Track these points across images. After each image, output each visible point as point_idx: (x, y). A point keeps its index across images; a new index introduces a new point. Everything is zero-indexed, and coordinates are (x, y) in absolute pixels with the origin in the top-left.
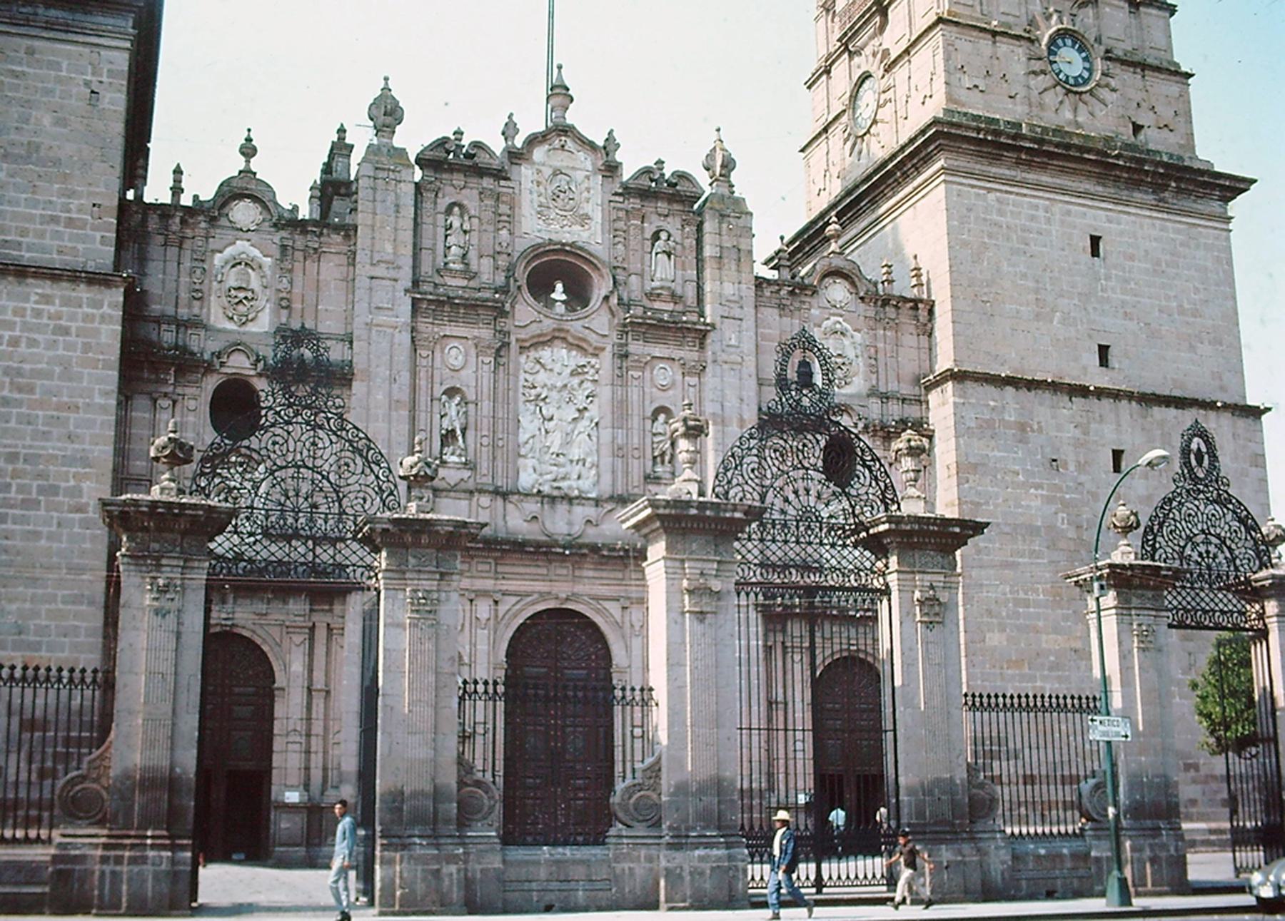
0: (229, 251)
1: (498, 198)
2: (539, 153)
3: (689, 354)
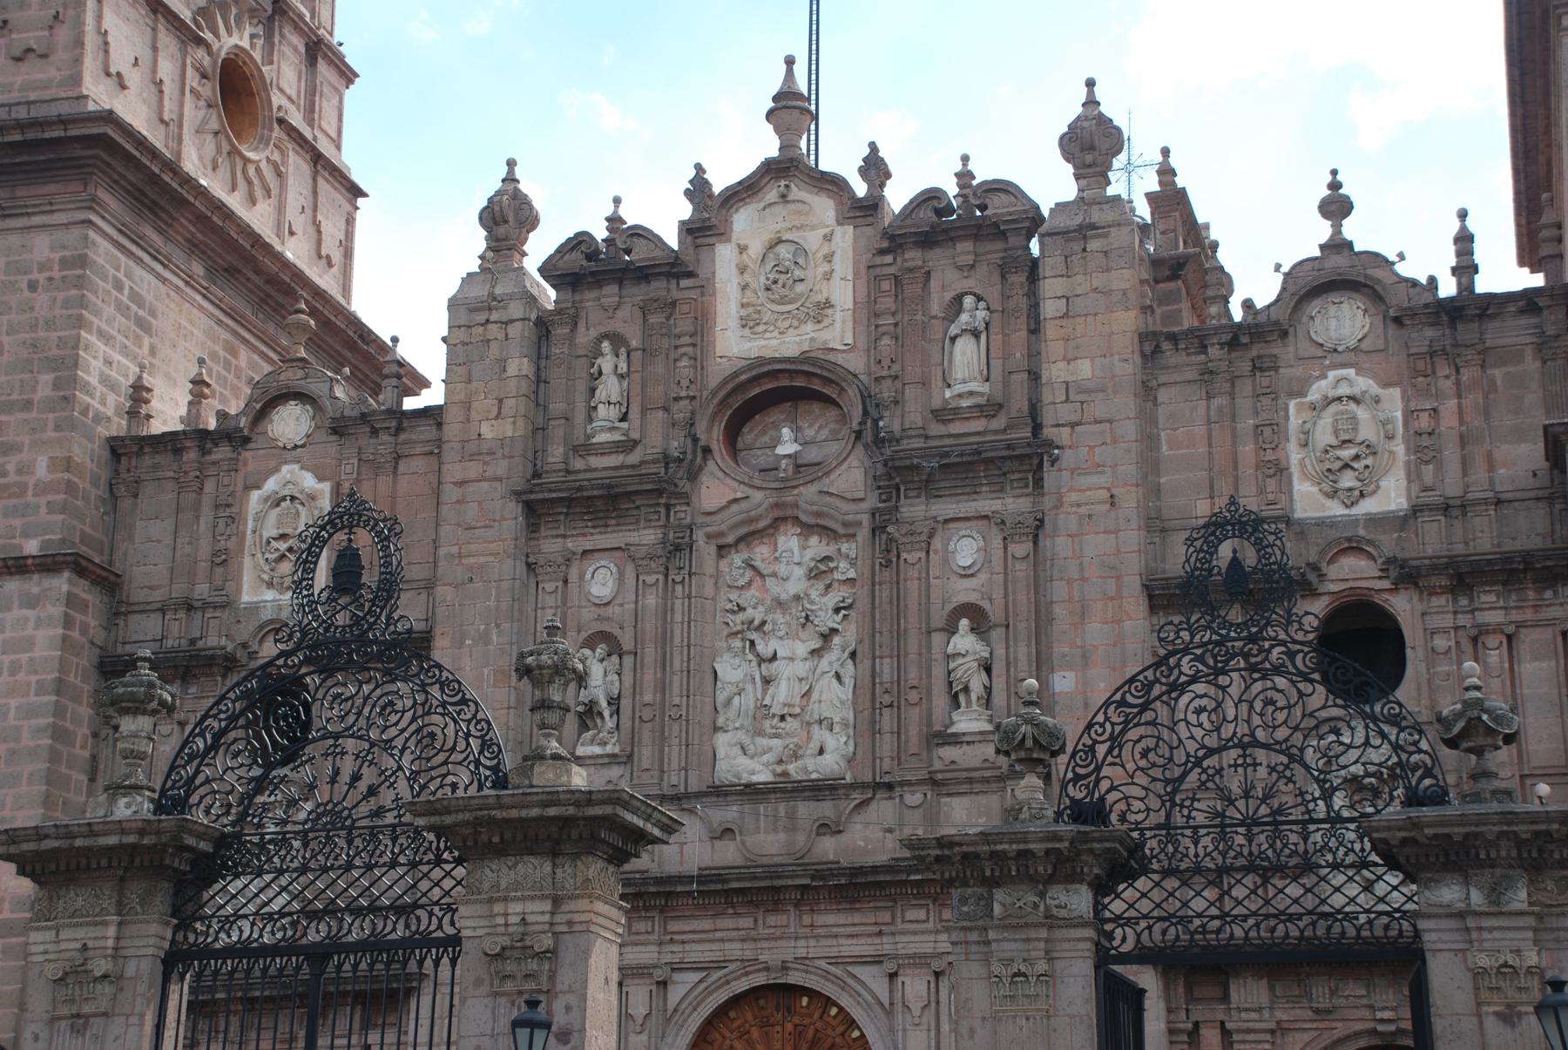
0: (271, 485)
2: (743, 221)
3: (1014, 504)
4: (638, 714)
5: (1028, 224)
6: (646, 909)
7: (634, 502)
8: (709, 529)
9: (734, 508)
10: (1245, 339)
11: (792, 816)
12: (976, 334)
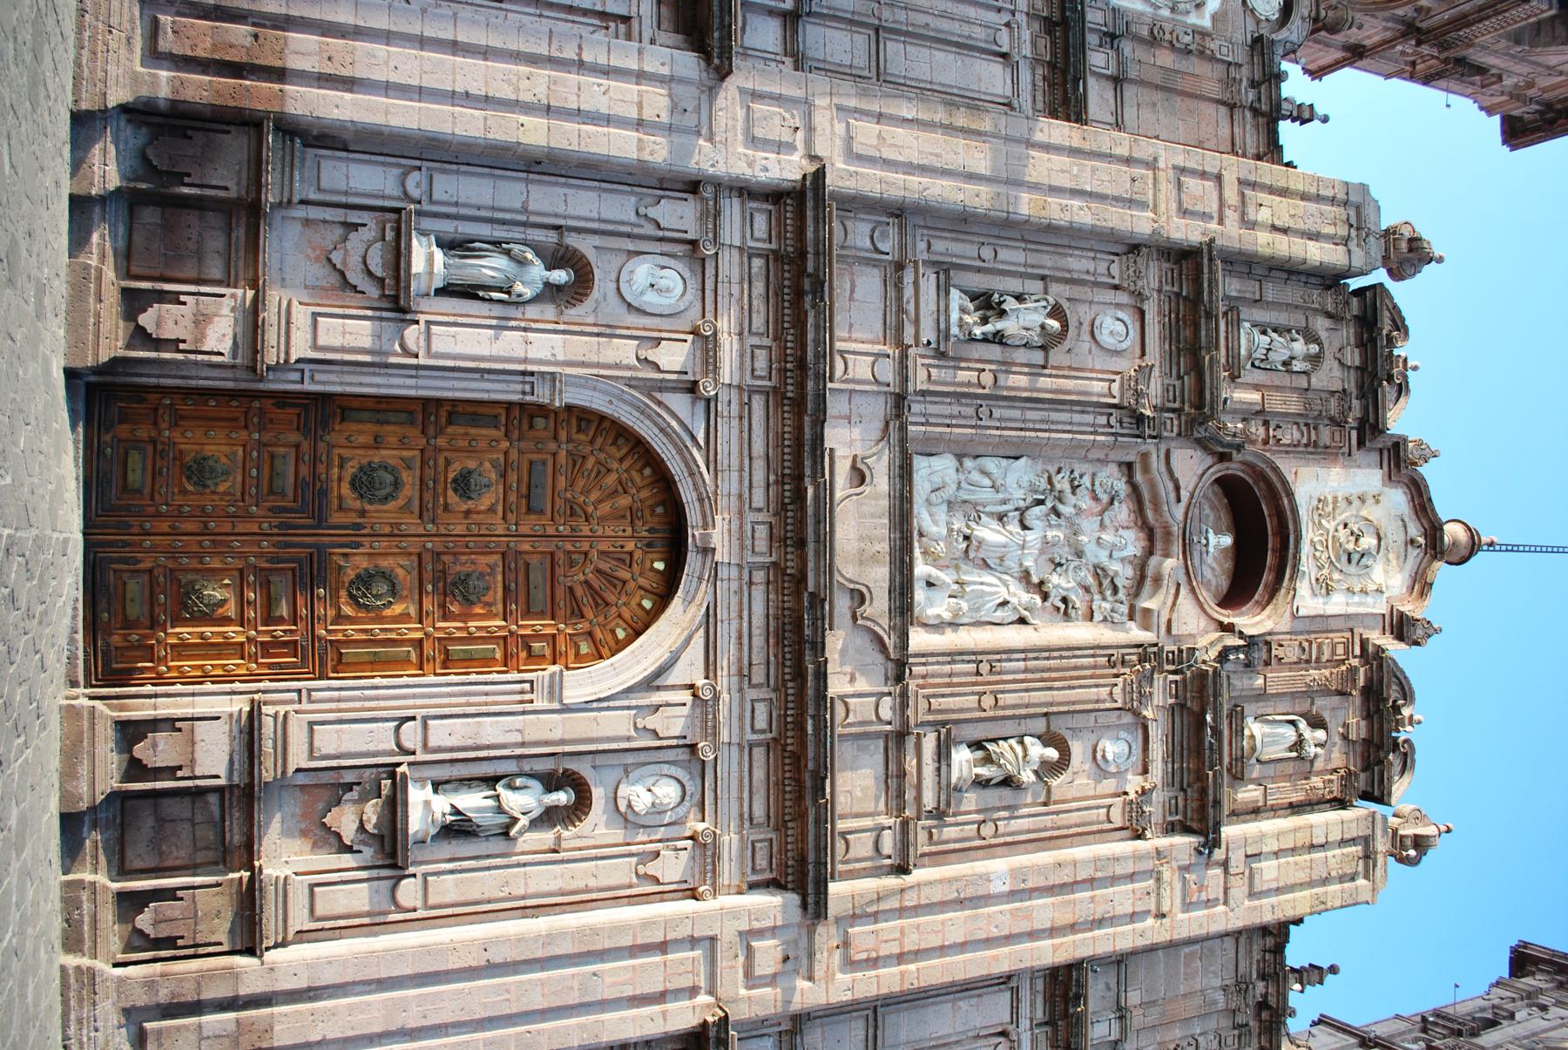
1: (1338, 423)
2: (1397, 499)
4: (987, 367)
5: (1376, 793)
6: (783, 371)
7: (1186, 374)
8: (1154, 457)
9: (1170, 486)
10: (1265, 1015)
11: (874, 559)
12: (1299, 744)
